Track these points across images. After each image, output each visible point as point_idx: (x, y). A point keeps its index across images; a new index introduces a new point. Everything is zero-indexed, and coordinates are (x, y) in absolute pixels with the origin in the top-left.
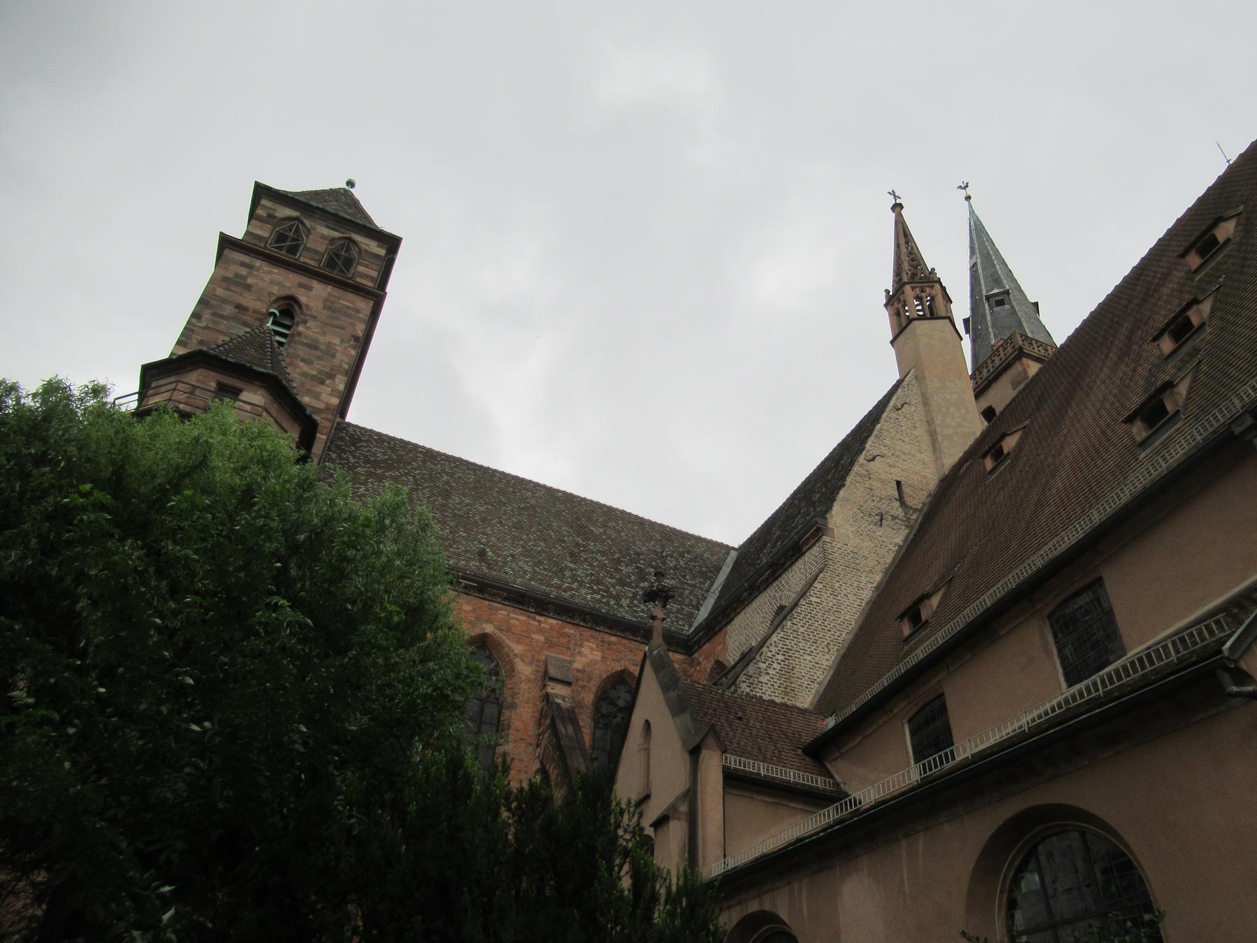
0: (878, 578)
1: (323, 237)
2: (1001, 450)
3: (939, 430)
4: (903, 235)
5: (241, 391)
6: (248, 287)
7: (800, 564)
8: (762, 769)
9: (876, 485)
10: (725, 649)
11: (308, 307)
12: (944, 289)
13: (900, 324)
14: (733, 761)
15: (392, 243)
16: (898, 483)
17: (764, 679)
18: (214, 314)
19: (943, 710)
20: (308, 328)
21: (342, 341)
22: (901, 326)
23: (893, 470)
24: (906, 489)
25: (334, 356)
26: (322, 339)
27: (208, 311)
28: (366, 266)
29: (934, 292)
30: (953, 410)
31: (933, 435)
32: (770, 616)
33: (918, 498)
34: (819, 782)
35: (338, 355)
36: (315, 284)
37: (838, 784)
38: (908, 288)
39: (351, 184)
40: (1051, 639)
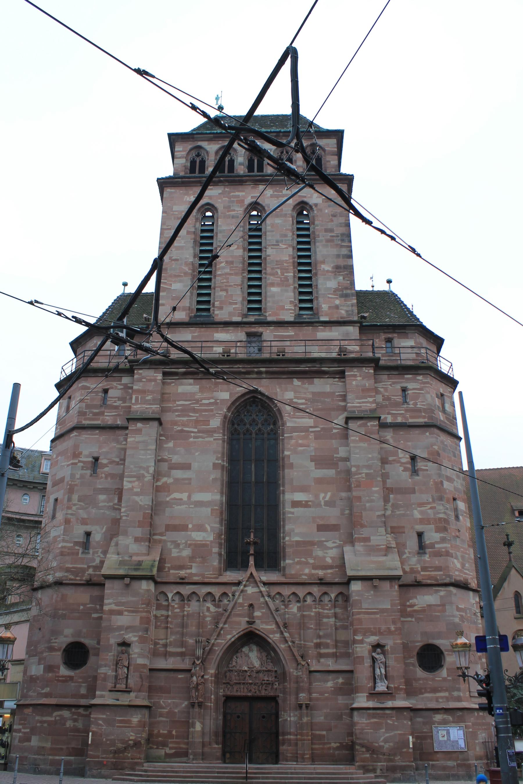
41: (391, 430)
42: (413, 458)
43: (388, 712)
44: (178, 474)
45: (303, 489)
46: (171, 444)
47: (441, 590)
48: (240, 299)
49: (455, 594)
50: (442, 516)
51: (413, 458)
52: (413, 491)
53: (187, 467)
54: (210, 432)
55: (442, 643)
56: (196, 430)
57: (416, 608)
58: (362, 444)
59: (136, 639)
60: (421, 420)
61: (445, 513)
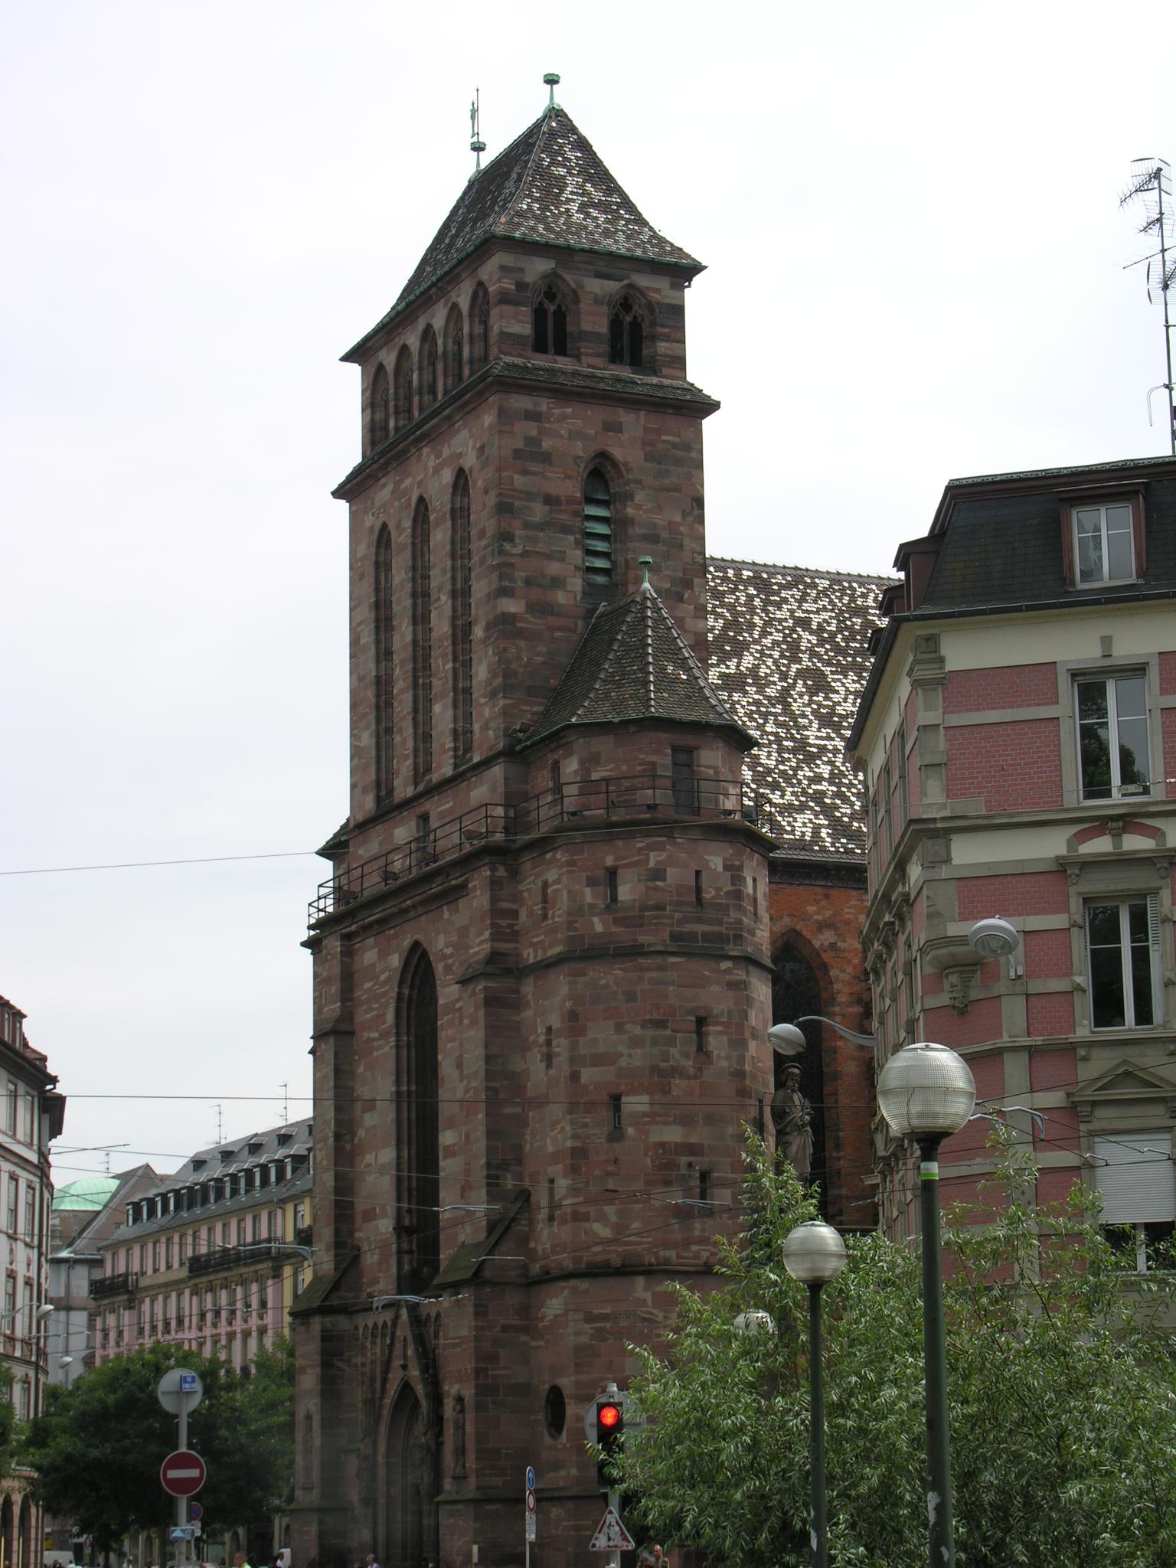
1: (597, 301)
5: (696, 749)
6: (546, 458)
11: (626, 464)
15: (684, 270)
18: (527, 526)
20: (639, 507)
21: (684, 515)
25: (681, 546)
26: (660, 520)
27: (517, 523)
28: (668, 338)
35: (686, 541)
36: (626, 417)
39: (551, 80)
41: (531, 980)
42: (549, 1029)
43: (460, 1507)
44: (369, 1119)
45: (451, 1126)
46: (361, 1070)
47: (564, 1288)
48: (410, 744)
49: (586, 1291)
50: (569, 1144)
51: (549, 1029)
52: (542, 1102)
53: (370, 1105)
54: (384, 1035)
55: (566, 1383)
56: (376, 1035)
57: (546, 1323)
58: (472, 1033)
59: (314, 1409)
60: (557, 950)
61: (575, 1137)
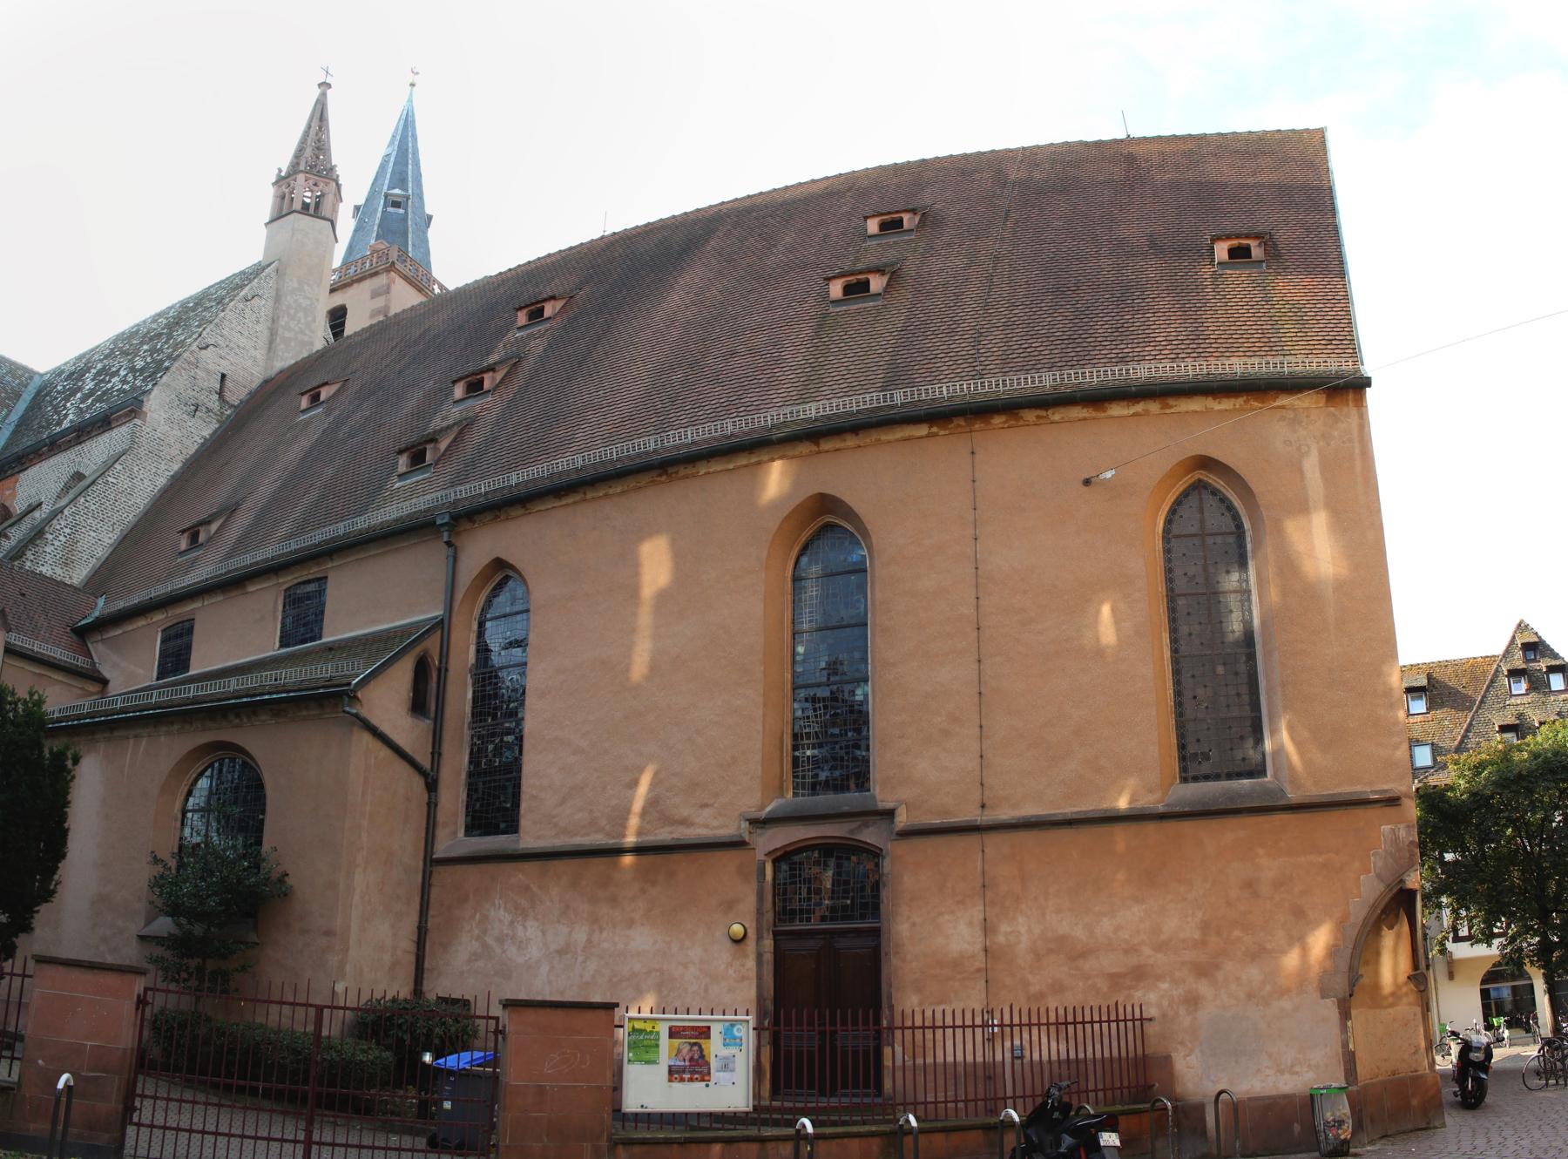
0: (176, 467)
2: (318, 394)
3: (280, 331)
4: (320, 115)
7: (105, 437)
8: (37, 647)
9: (201, 374)
10: (14, 495)
12: (338, 186)
13: (281, 209)
14: (17, 640)
16: (223, 376)
17: (48, 549)
19: (190, 631)
22: (283, 209)
23: (222, 362)
24: (228, 383)
29: (326, 190)
30: (300, 315)
31: (273, 333)
32: (65, 478)
33: (236, 395)
34: (81, 662)
37: (94, 663)
38: (301, 177)
40: (280, 608)
